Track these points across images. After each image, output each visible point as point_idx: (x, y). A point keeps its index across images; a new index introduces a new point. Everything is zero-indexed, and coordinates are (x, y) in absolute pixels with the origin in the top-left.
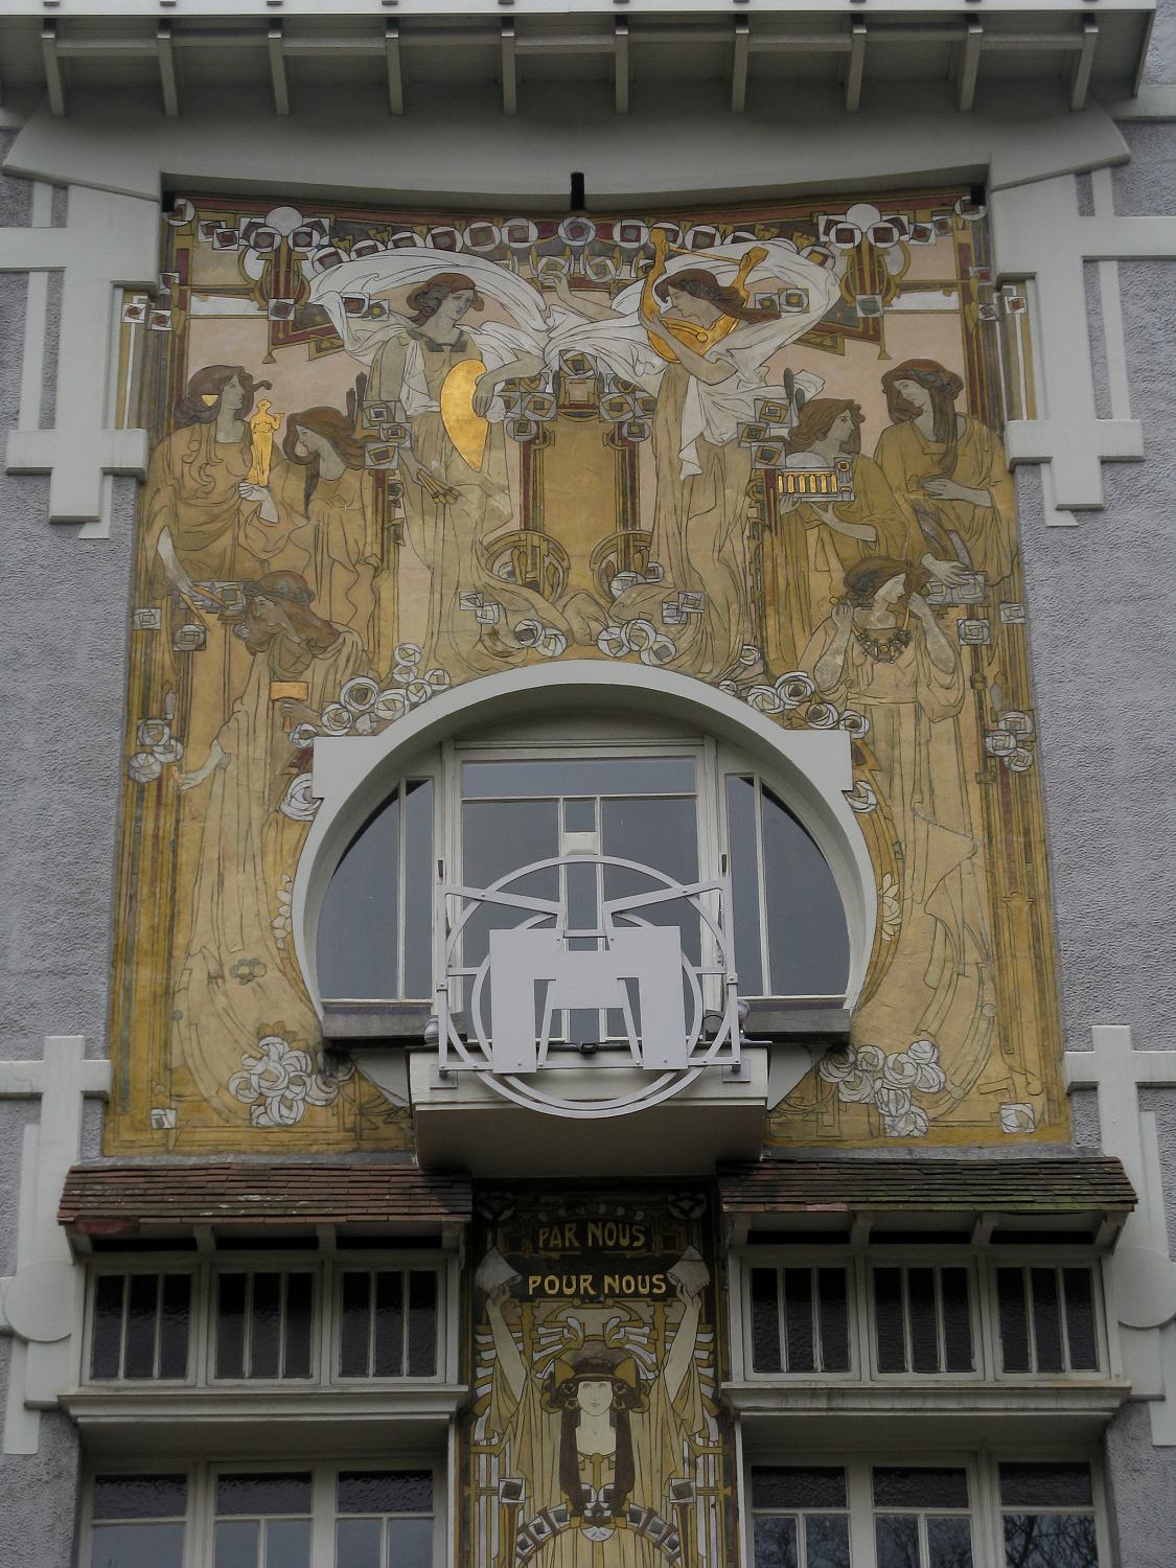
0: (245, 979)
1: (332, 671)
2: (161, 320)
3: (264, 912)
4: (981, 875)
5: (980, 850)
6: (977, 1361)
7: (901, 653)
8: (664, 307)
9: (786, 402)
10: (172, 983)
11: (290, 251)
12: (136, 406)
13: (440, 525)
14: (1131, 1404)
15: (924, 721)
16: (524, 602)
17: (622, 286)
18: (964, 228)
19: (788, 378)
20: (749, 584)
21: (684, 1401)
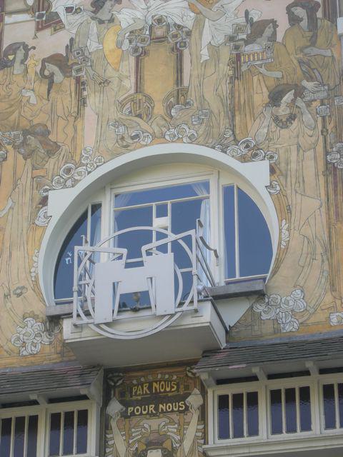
0: (19, 295)
3: (27, 265)
4: (324, 215)
5: (324, 204)
7: (292, 123)
13: (102, 95)
19: (247, 13)
20: (229, 103)
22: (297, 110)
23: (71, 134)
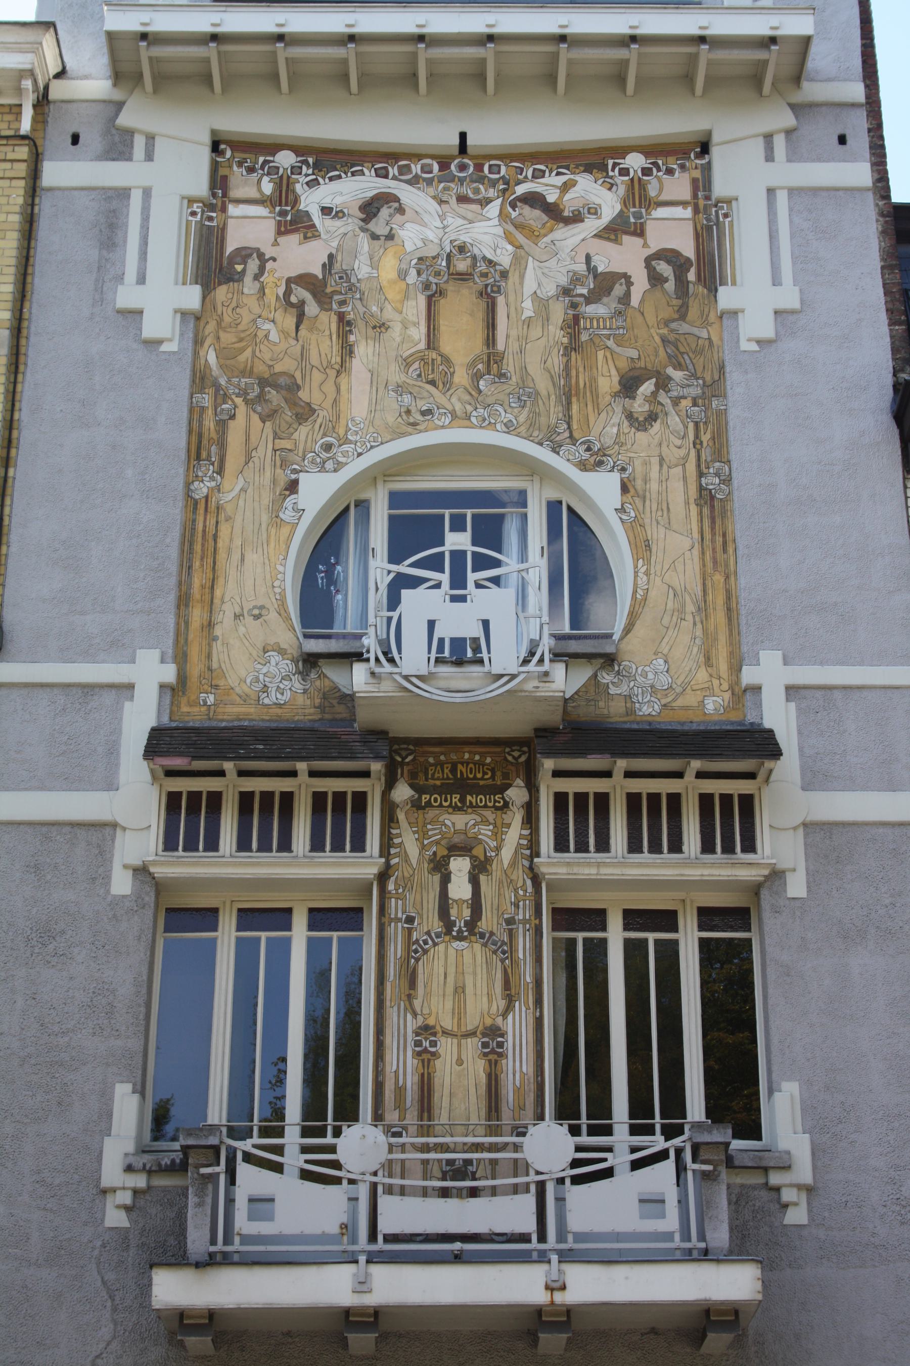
0: (257, 617)
1: (311, 433)
2: (210, 219)
3: (268, 577)
5: (696, 544)
6: (685, 848)
7: (652, 426)
8: (514, 214)
9: (586, 273)
10: (213, 619)
11: (289, 177)
12: (195, 271)
13: (377, 345)
14: (777, 875)
15: (665, 467)
16: (426, 393)
17: (488, 201)
18: (696, 168)
19: (588, 258)
21: (512, 869)
22: (660, 407)
23: (331, 395)
